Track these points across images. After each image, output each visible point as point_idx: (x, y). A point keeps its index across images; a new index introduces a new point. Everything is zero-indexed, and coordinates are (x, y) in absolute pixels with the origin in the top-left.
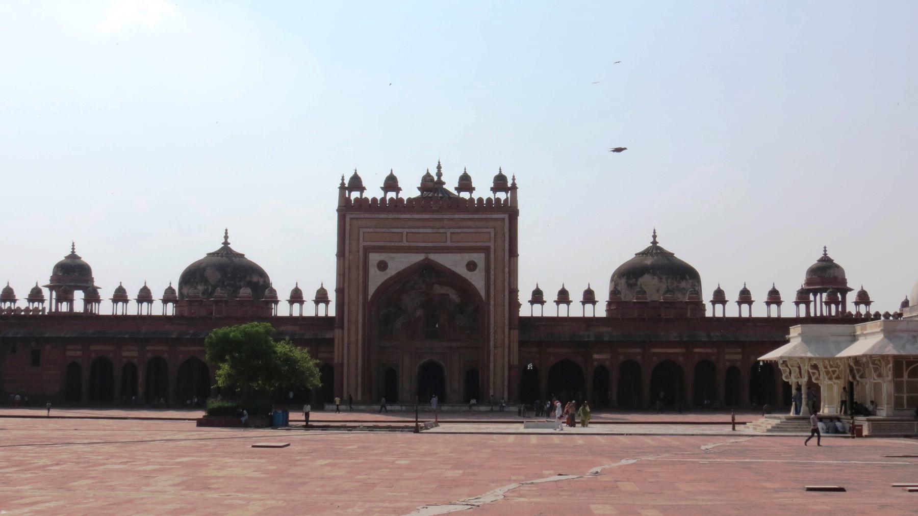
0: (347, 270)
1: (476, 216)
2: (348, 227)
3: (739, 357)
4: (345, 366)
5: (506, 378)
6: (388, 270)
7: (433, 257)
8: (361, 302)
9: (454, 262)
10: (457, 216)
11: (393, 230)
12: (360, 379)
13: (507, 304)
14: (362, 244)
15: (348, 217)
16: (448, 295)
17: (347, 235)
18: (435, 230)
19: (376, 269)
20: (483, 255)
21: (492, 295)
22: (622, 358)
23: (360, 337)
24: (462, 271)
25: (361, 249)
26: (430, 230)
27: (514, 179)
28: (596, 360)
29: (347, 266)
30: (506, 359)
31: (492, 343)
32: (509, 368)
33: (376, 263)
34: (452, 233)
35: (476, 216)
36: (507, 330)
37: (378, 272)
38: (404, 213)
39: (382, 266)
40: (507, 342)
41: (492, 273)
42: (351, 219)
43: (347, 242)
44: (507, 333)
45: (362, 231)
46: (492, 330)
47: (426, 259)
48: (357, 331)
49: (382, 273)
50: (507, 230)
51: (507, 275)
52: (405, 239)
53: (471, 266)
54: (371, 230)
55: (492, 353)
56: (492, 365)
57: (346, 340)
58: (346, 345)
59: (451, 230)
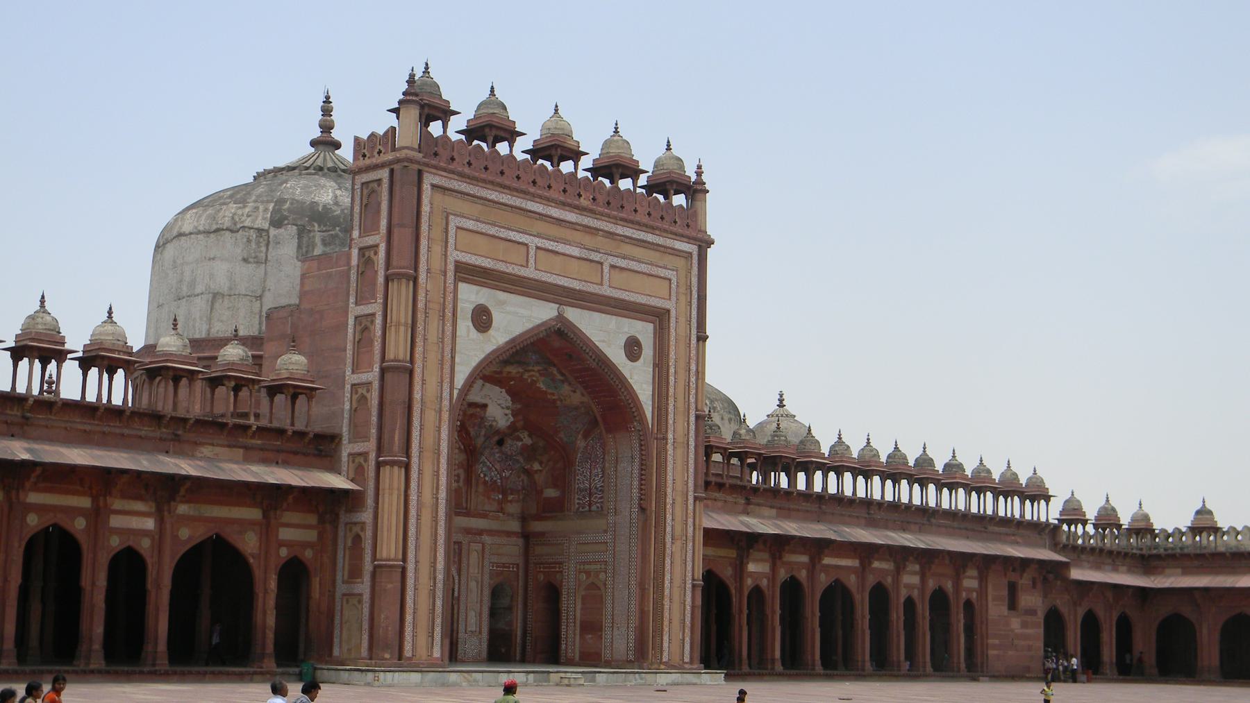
0: (420, 316)
1: (650, 237)
2: (426, 208)
3: (915, 580)
4: (411, 567)
5: (688, 608)
6: (491, 332)
7: (574, 315)
8: (446, 403)
9: (605, 334)
10: (620, 230)
11: (513, 235)
12: (439, 603)
13: (692, 443)
14: (454, 255)
15: (429, 179)
16: (485, 406)
17: (424, 227)
18: (585, 254)
19: (470, 324)
20: (651, 326)
21: (671, 422)
22: (783, 574)
23: (443, 495)
24: (616, 355)
25: (451, 267)
26: (575, 251)
27: (699, 174)
28: (751, 574)
29: (421, 305)
30: (689, 568)
31: (669, 529)
32: (694, 586)
33: (470, 307)
34: (613, 267)
35: (650, 237)
36: (691, 500)
37: (474, 333)
38: (533, 197)
39: (482, 319)
40: (690, 530)
41: (672, 370)
42: (434, 186)
43: (424, 243)
44: (691, 507)
45: (454, 222)
46: (669, 500)
47: (560, 317)
48: (437, 474)
49: (480, 336)
50: (694, 280)
51: (693, 379)
52: (532, 261)
53: (633, 348)
54: (470, 224)
55: (668, 552)
56: (668, 577)
57: (413, 497)
58: (413, 512)
59: (610, 258)
